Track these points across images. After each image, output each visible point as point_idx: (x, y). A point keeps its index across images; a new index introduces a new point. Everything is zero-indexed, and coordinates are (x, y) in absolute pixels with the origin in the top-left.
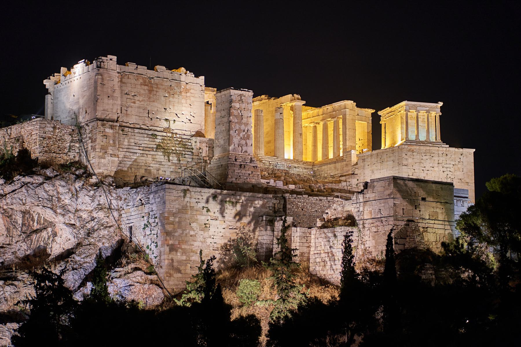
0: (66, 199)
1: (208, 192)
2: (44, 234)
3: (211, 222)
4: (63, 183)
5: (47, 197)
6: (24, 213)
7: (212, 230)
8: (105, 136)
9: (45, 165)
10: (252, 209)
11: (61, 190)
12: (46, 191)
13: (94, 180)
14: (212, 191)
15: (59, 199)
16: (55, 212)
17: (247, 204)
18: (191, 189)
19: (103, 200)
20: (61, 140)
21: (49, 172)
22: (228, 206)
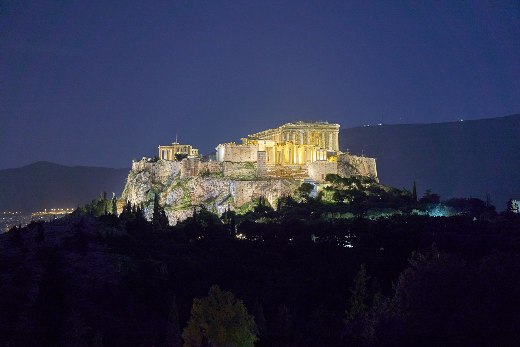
1: (247, 182)
9: (212, 174)
22: (253, 185)
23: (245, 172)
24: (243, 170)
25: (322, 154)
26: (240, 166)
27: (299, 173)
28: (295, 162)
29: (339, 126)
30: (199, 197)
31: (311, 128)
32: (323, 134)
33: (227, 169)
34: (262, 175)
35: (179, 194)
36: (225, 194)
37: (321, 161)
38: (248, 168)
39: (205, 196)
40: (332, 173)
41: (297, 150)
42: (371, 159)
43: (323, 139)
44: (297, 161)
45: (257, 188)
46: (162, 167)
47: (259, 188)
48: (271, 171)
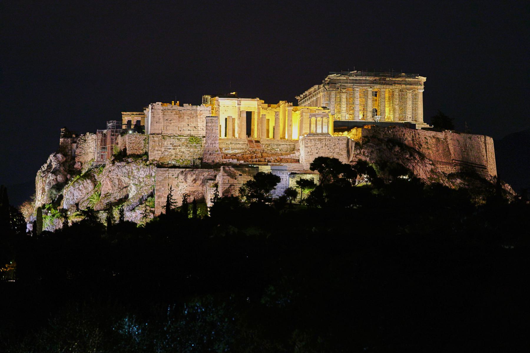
1: (178, 171)
2: (129, 188)
3: (179, 184)
4: (134, 165)
5: (126, 172)
7: (180, 187)
10: (202, 177)
11: (133, 168)
12: (126, 169)
13: (148, 163)
14: (181, 170)
15: (132, 172)
16: (130, 179)
17: (199, 175)
18: (170, 169)
21: (130, 160)
22: (189, 176)
23: (187, 153)
24: (183, 150)
25: (319, 123)
26: (176, 143)
27: (286, 157)
28: (286, 137)
29: (424, 79)
30: (107, 195)
31: (374, 82)
32: (396, 93)
34: (209, 159)
35: (84, 191)
37: (318, 134)
38: (191, 147)
39: (115, 195)
40: (324, 155)
41: (290, 116)
43: (397, 102)
44: (290, 135)
45: (195, 180)
46: (85, 145)
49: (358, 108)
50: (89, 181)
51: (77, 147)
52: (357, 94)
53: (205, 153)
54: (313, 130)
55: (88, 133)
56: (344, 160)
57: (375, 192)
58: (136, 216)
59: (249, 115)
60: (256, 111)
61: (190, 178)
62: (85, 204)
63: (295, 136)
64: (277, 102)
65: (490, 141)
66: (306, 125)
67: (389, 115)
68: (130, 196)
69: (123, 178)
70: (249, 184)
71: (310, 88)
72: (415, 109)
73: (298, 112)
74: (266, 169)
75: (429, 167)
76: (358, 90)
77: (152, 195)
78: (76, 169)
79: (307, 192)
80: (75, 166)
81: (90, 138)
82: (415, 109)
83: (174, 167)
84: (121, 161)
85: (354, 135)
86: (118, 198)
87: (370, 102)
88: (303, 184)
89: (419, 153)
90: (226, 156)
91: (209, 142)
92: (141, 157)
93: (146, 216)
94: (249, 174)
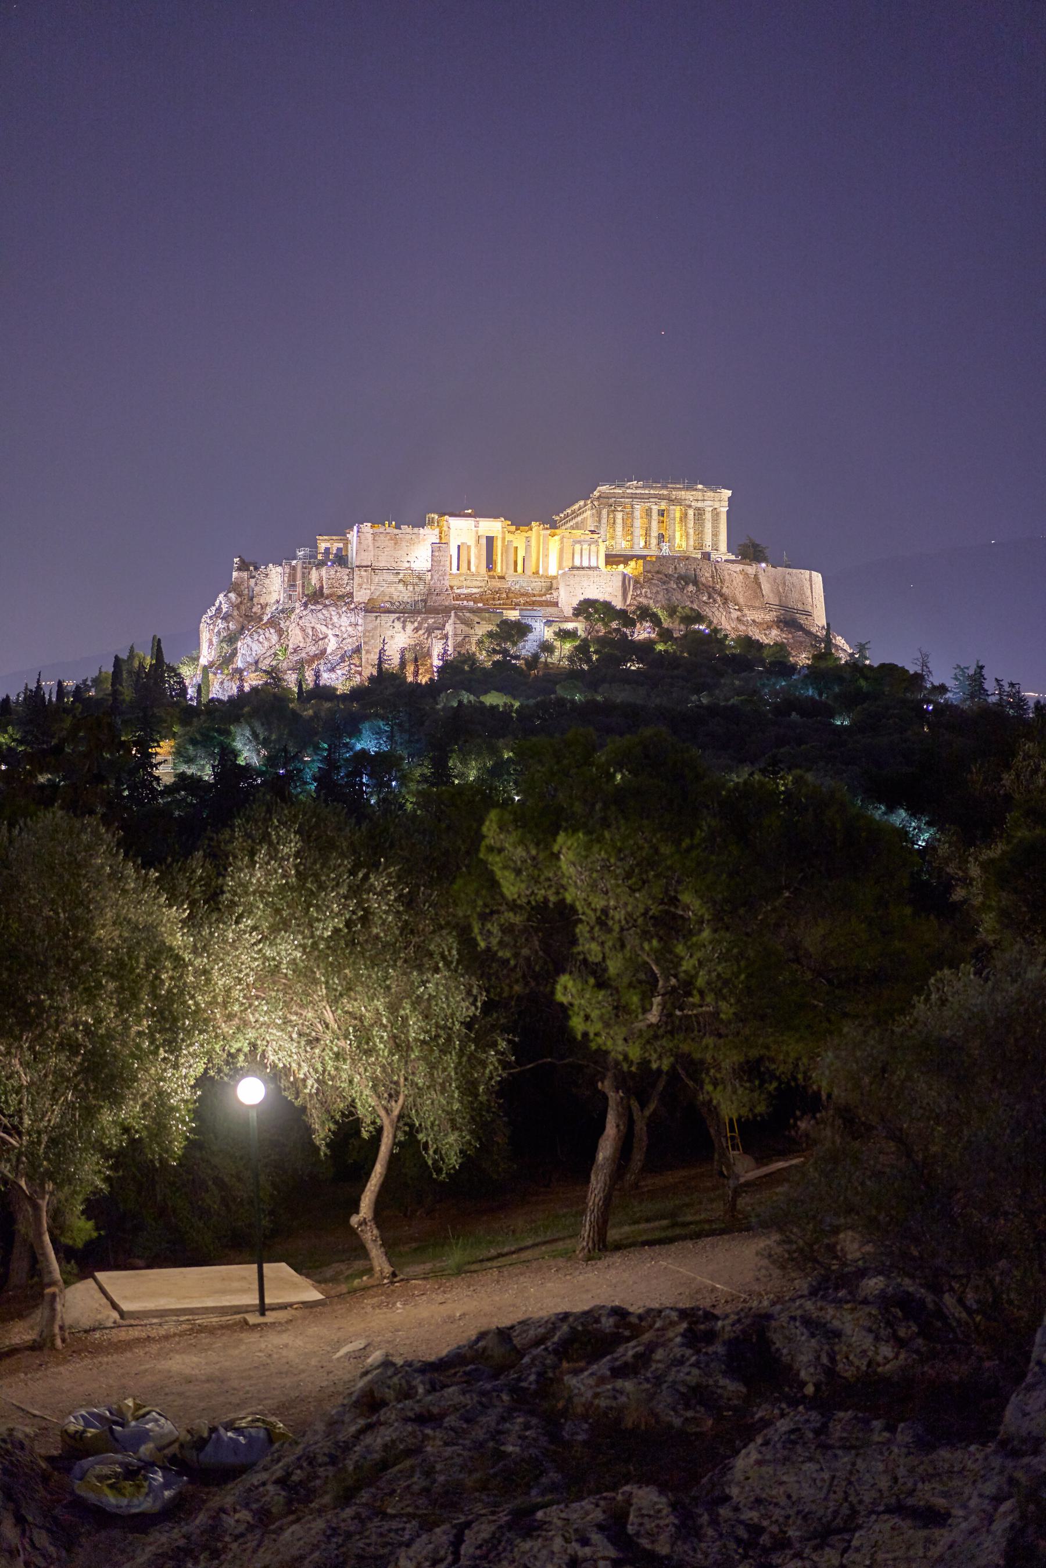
0: (335, 619)
6: (313, 628)
8: (361, 577)
13: (352, 606)
19: (353, 620)
20: (341, 579)
21: (327, 602)
25: (585, 553)
26: (391, 578)
28: (541, 572)
29: (729, 493)
31: (661, 498)
33: (360, 585)
34: (434, 601)
36: (349, 646)
39: (308, 649)
42: (803, 571)
43: (691, 524)
44: (546, 569)
45: (416, 630)
46: (267, 581)
47: (421, 632)
48: (468, 591)
49: (639, 531)
50: (272, 631)
51: (256, 584)
52: (637, 514)
53: (430, 593)
54: (577, 563)
55: (271, 565)
56: (618, 604)
57: (660, 647)
58: (337, 680)
59: (490, 540)
60: (500, 536)
61: (410, 627)
62: (267, 662)
63: (553, 571)
64: (528, 524)
65: (817, 578)
66: (567, 556)
67: (681, 542)
68: (329, 651)
69: (318, 626)
70: (490, 635)
71: (573, 504)
72: (715, 535)
73: (557, 538)
74: (513, 615)
75: (735, 614)
76: (639, 509)
77: (358, 650)
78: (255, 613)
79: (568, 646)
80: (254, 610)
81: (274, 571)
82: (715, 535)
83: (389, 611)
84: (317, 603)
85: (632, 569)
86: (311, 654)
87: (654, 524)
88: (565, 635)
89: (721, 595)
90: (458, 597)
91: (435, 577)
92: (344, 599)
93: (349, 679)
94: (489, 621)
